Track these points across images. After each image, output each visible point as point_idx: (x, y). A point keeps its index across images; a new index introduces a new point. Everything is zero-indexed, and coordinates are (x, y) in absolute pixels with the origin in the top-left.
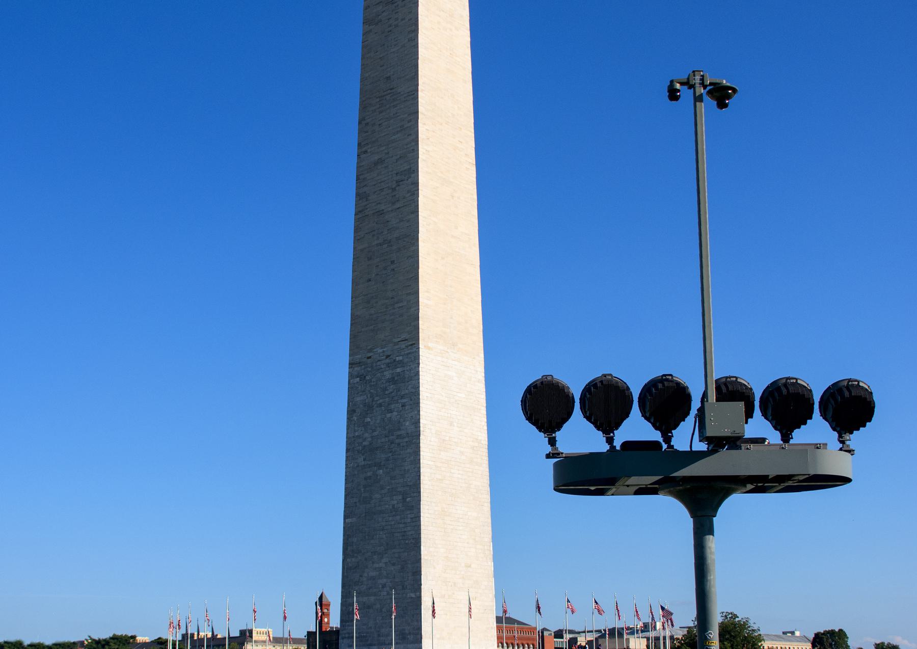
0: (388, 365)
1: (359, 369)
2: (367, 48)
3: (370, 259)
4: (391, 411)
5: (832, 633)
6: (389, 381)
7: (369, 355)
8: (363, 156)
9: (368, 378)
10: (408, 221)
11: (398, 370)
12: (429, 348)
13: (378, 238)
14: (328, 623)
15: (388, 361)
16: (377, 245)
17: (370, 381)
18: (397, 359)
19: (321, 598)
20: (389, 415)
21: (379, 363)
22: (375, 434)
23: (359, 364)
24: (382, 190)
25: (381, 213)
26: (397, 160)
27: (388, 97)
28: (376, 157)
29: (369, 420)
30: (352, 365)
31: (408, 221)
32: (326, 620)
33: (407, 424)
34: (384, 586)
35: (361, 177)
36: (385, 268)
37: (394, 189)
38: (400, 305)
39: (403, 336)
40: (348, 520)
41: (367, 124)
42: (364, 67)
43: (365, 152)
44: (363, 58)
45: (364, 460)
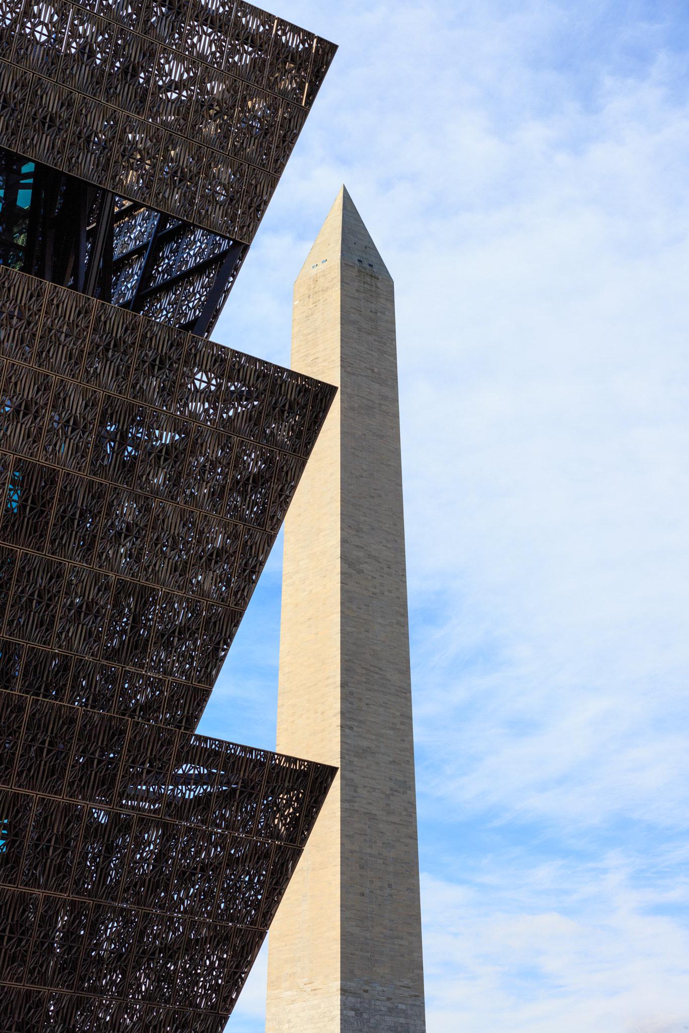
0: (390, 1010)
1: (353, 1000)
3: (362, 868)
8: (348, 731)
9: (365, 1016)
10: (406, 845)
13: (371, 847)
15: (388, 1004)
16: (371, 855)
18: (401, 1006)
21: (378, 1003)
23: (354, 994)
24: (374, 789)
25: (372, 817)
26: (390, 762)
27: (377, 676)
28: (365, 744)
35: (347, 757)
36: (381, 888)
37: (388, 796)
38: (402, 942)
39: (406, 982)
41: (351, 693)
43: (351, 728)
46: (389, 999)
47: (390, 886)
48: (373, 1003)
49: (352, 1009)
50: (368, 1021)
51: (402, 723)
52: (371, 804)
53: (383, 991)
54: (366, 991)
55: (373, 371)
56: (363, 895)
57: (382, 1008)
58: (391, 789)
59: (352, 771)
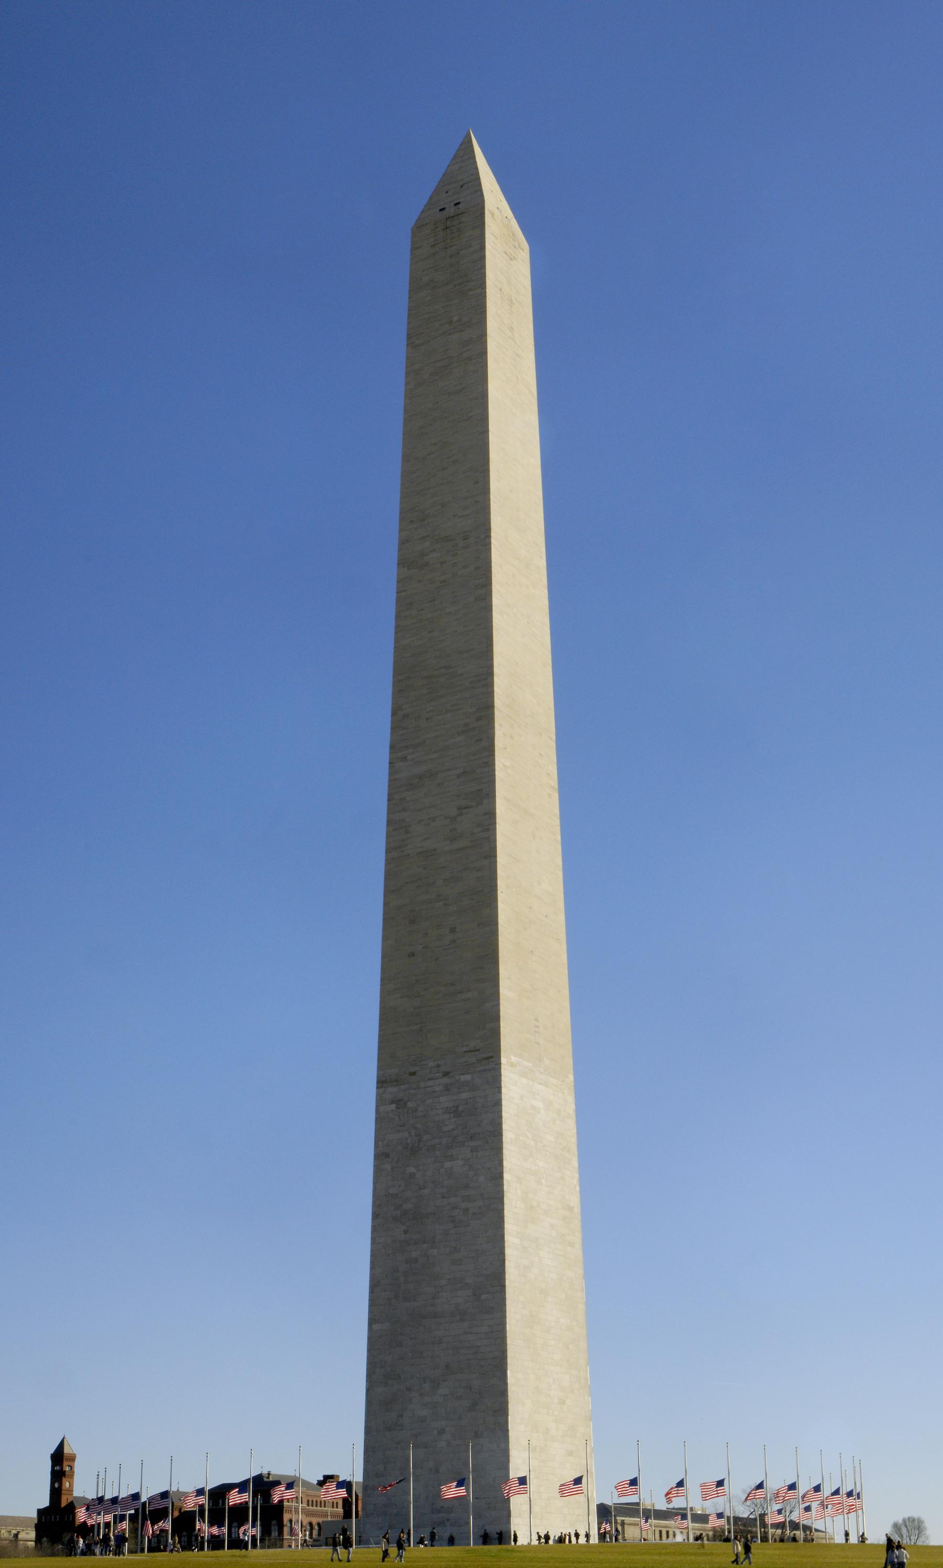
0: (447, 1088)
1: (395, 1089)
2: (405, 604)
5: (912, 1520)
7: (412, 1069)
9: (410, 1104)
11: (464, 1096)
12: (512, 1065)
14: (71, 1490)
15: (446, 1080)
19: (61, 1446)
20: (448, 1164)
21: (431, 1083)
23: (397, 1081)
26: (459, 776)
29: (412, 1170)
30: (382, 1083)
32: (67, 1485)
33: (481, 1179)
34: (441, 1432)
40: (375, 1327)
42: (399, 629)
43: (404, 759)
44: (398, 617)
45: (405, 1232)
46: (446, 1074)
47: (453, 930)
48: (422, 1085)
49: (392, 1102)
51: (477, 720)
52: (429, 838)
53: (438, 1066)
54: (413, 1074)
55: (451, 322)
56: (412, 955)
57: (437, 1089)
58: (460, 808)
59: (404, 810)
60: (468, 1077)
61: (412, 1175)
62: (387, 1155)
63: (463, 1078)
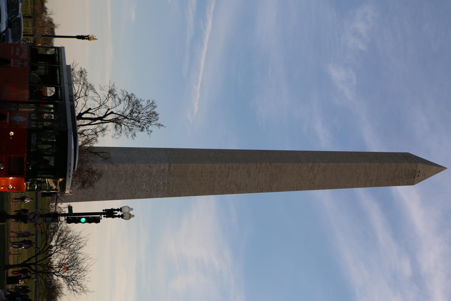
0: (165, 183)
4: (146, 185)
6: (159, 183)
9: (162, 174)
10: (219, 190)
15: (167, 183)
17: (161, 175)
18: (166, 188)
20: (145, 184)
22: (139, 179)
23: (169, 169)
29: (145, 175)
31: (219, 190)
41: (268, 168)
43: (256, 168)
46: (168, 183)
47: (205, 183)
49: (164, 168)
50: (161, 175)
51: (260, 189)
54: (170, 174)
55: (380, 176)
56: (202, 173)
60: (166, 189)
61: (144, 175)
62: (150, 168)
63: (166, 188)
